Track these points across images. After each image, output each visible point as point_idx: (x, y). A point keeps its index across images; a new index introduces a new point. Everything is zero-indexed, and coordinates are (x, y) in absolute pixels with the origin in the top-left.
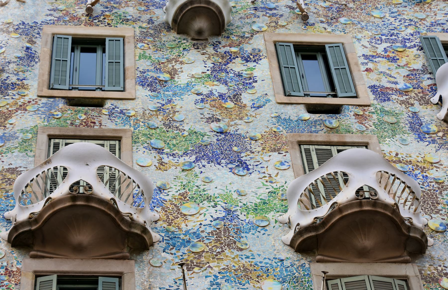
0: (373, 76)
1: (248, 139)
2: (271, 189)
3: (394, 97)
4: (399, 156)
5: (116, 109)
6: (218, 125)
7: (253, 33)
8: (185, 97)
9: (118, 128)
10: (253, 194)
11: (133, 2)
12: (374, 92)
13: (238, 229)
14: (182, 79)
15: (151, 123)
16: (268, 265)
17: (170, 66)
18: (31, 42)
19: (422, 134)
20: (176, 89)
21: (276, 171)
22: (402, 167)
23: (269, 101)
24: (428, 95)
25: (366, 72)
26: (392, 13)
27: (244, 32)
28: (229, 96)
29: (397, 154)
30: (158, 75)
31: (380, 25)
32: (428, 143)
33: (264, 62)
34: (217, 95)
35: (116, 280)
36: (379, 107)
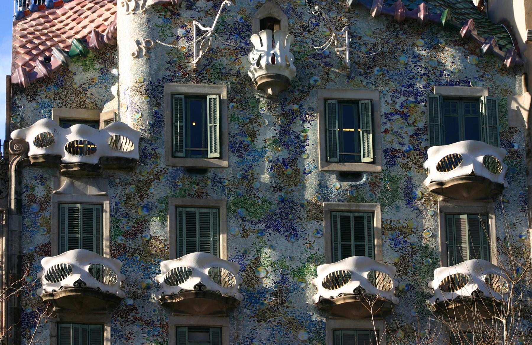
0: (389, 137)
1: (299, 206)
2: (310, 255)
3: (399, 160)
4: (392, 224)
5: (216, 178)
6: (280, 194)
7: (311, 87)
10: (298, 259)
11: (226, 51)
12: (386, 156)
13: (287, 290)
14: (259, 143)
15: (239, 191)
16: (302, 319)
17: (251, 127)
18: (158, 105)
20: (255, 154)
22: (392, 235)
24: (422, 158)
25: (384, 134)
26: (415, 57)
28: (289, 162)
29: (391, 222)
30: (243, 139)
31: (403, 73)
32: (413, 209)
35: (219, 330)
36: (387, 172)
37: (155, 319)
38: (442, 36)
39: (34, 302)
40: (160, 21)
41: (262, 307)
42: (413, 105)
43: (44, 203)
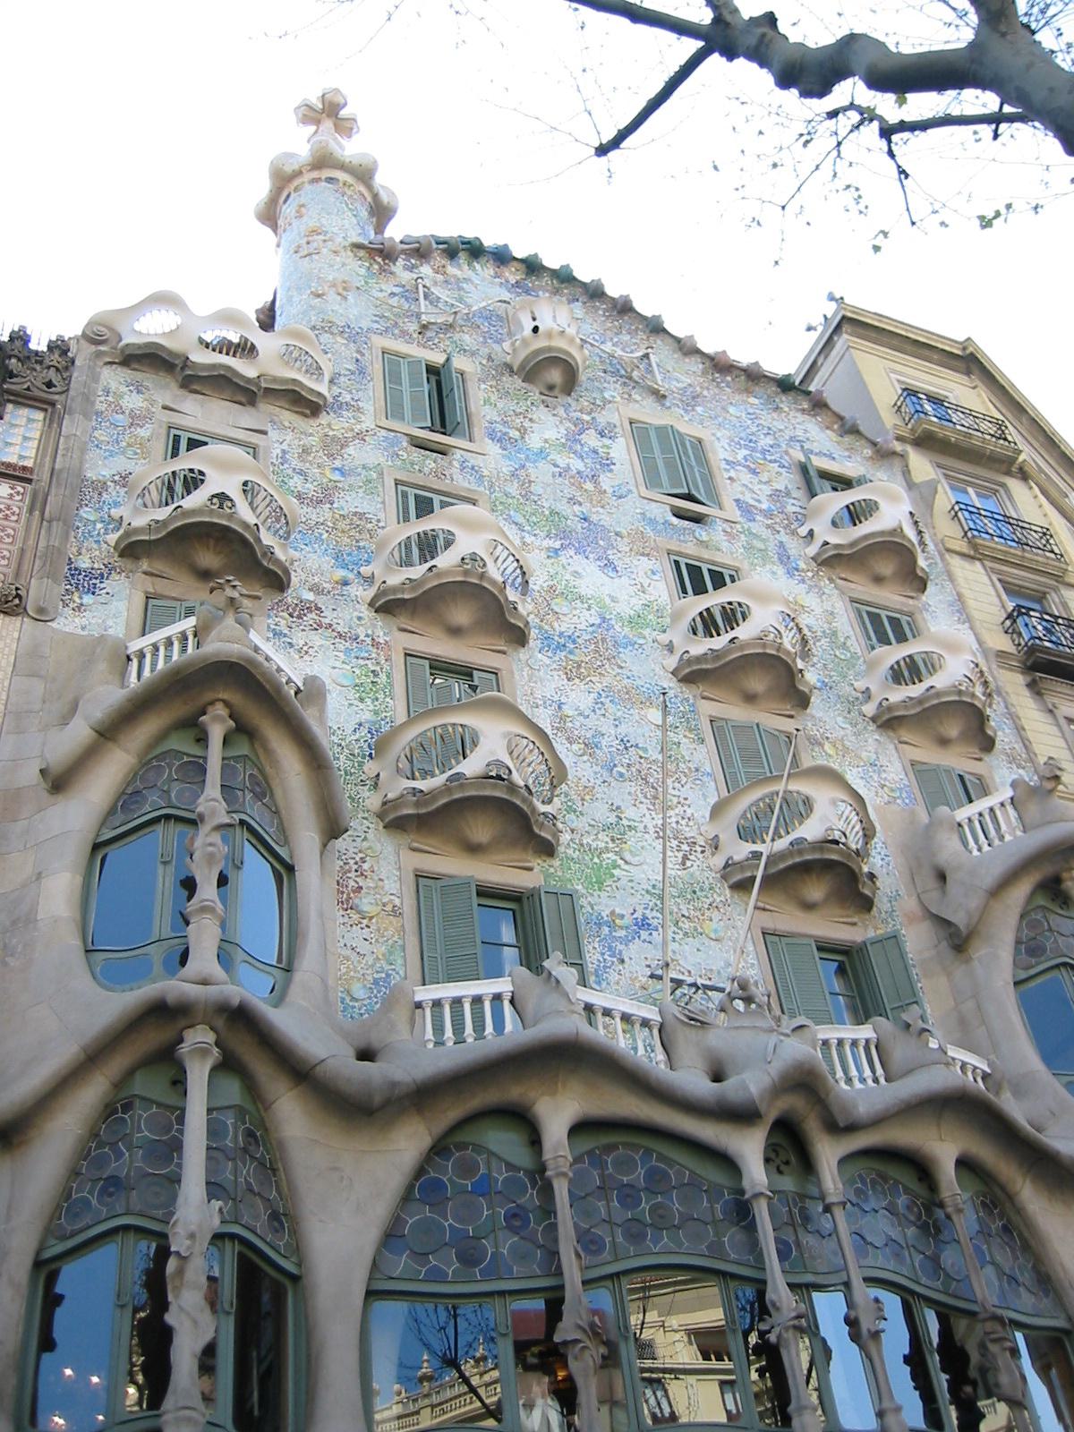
0: (737, 487)
7: (606, 402)
8: (540, 465)
9: (473, 487)
12: (740, 508)
14: (534, 441)
15: (508, 490)
17: (518, 421)
18: (358, 352)
19: (792, 571)
20: (528, 452)
21: (648, 581)
23: (630, 491)
27: (595, 399)
33: (621, 440)
34: (575, 471)
36: (746, 527)
37: (361, 632)
38: (782, 402)
39: (97, 553)
40: (363, 271)
41: (572, 657)
42: (762, 462)
43: (136, 419)
